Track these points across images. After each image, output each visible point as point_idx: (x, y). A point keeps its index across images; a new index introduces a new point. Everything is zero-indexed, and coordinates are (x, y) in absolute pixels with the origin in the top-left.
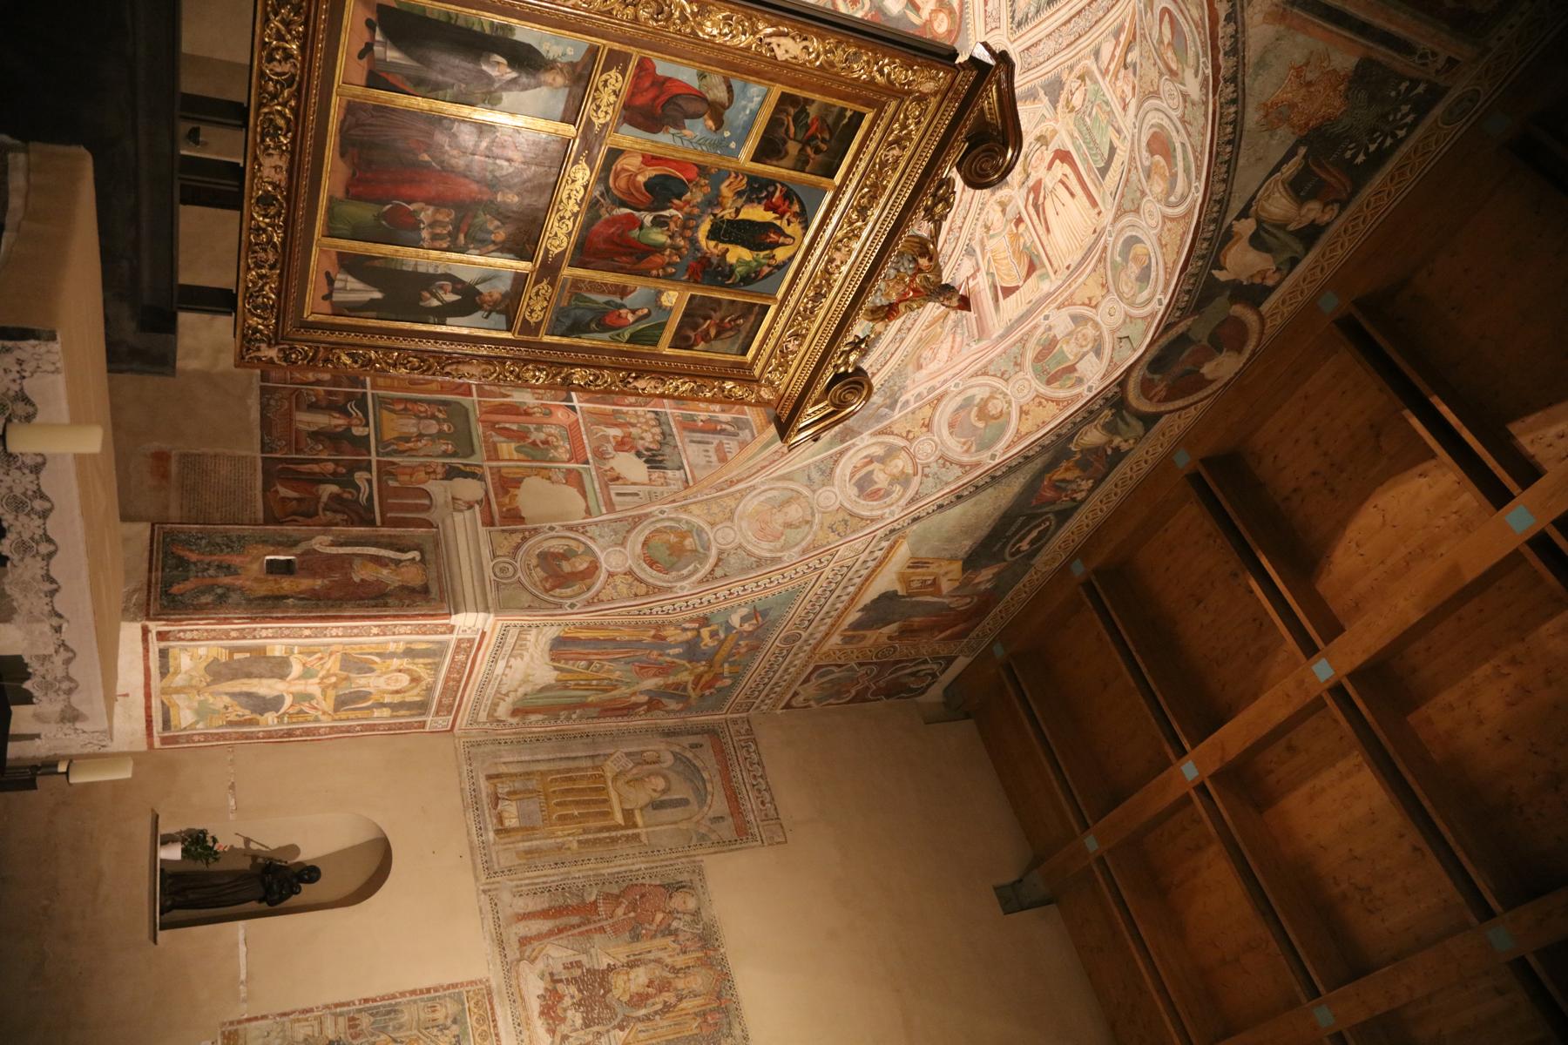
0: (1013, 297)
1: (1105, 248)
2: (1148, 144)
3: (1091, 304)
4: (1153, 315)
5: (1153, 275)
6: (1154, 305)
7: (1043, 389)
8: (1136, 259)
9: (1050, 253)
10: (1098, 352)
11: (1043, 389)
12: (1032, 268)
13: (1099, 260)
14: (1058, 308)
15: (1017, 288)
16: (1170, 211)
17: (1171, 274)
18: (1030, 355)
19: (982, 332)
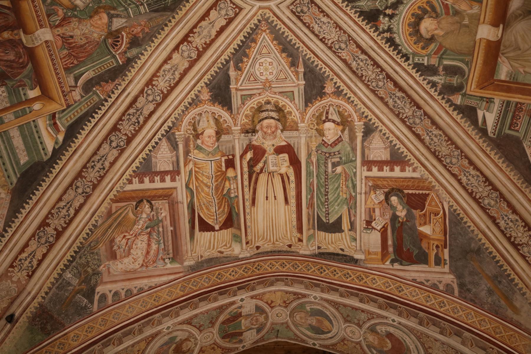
0: (208, 234)
1: (304, 296)
2: (391, 334)
3: (271, 305)
4: (303, 341)
5: (323, 336)
6: (311, 342)
7: (219, 341)
8: (318, 321)
9: (248, 224)
10: (259, 331)
11: (219, 341)
12: (229, 222)
13: (295, 294)
14: (252, 297)
15: (210, 229)
16: (365, 348)
17: (333, 349)
18: (222, 318)
19: (176, 255)
